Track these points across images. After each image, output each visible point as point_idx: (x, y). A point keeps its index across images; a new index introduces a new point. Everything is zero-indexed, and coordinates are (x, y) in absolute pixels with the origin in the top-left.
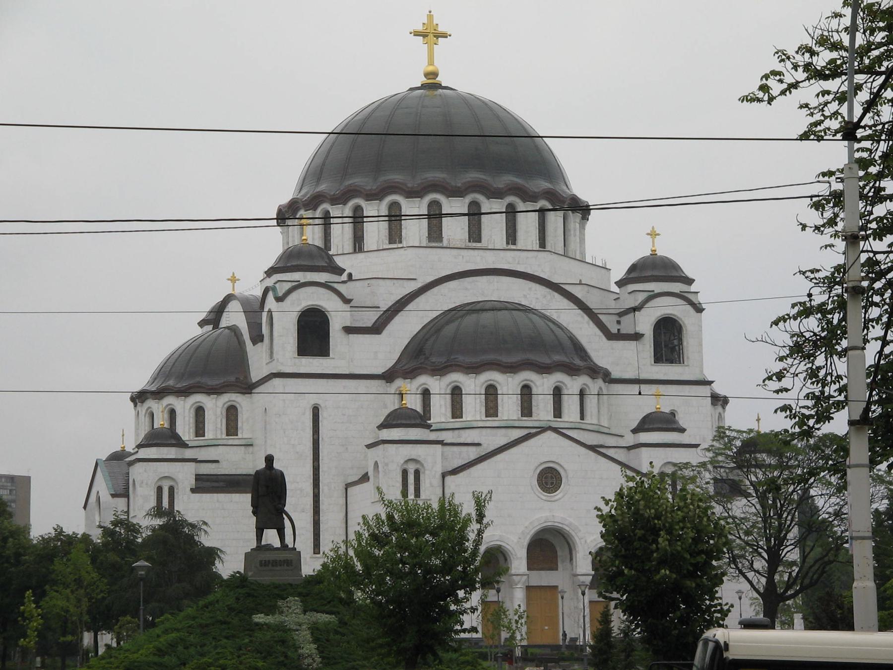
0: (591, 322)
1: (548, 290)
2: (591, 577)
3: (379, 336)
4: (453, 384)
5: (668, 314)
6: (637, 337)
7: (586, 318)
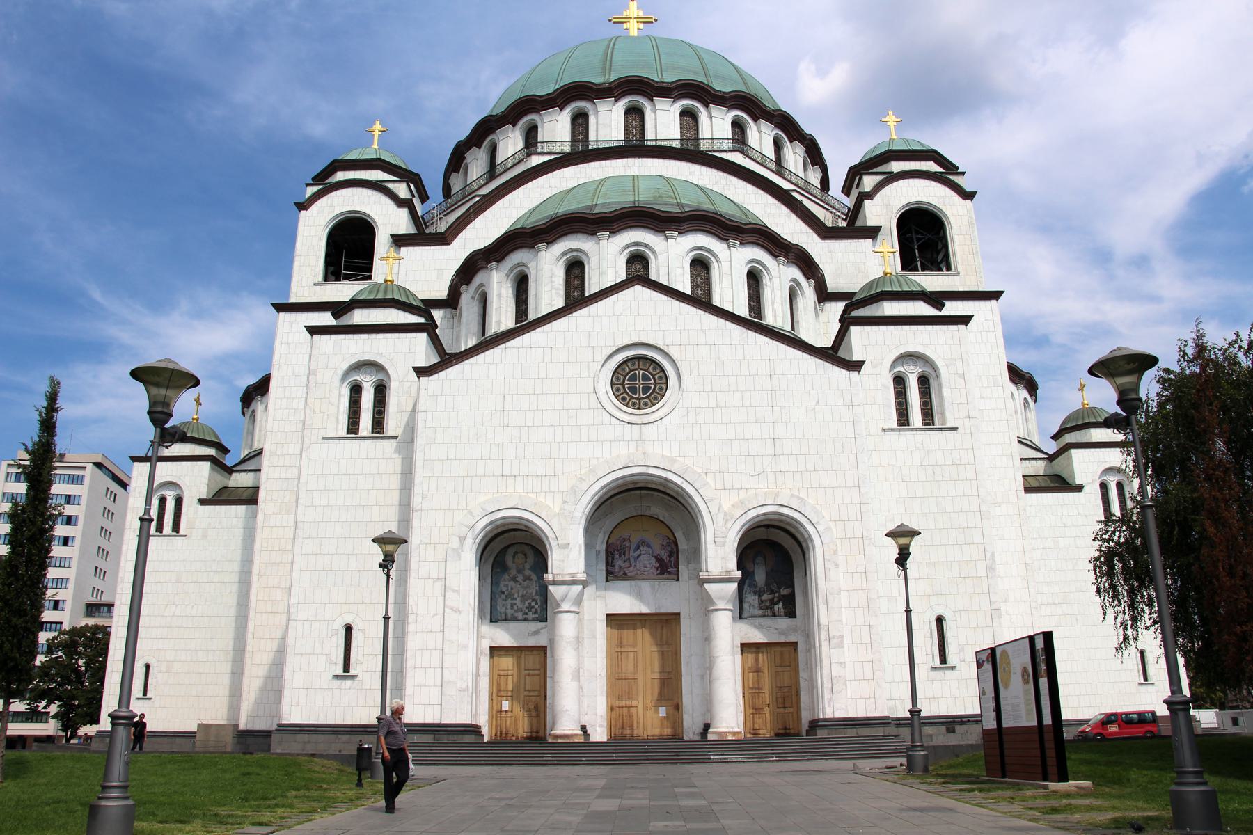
0: (794, 217)
1: (721, 173)
2: (735, 585)
3: (449, 247)
4: (515, 272)
5: (917, 203)
6: (872, 233)
7: (785, 210)
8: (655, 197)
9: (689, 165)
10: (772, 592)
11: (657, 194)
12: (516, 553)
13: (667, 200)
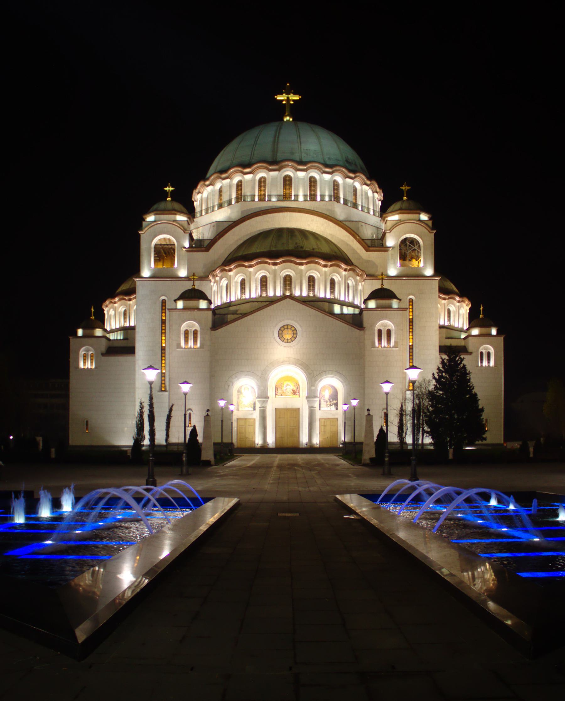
1: (325, 220)
7: (351, 237)
8: (295, 247)
9: (311, 216)
10: (331, 402)
11: (296, 246)
12: (245, 388)
13: (299, 249)
